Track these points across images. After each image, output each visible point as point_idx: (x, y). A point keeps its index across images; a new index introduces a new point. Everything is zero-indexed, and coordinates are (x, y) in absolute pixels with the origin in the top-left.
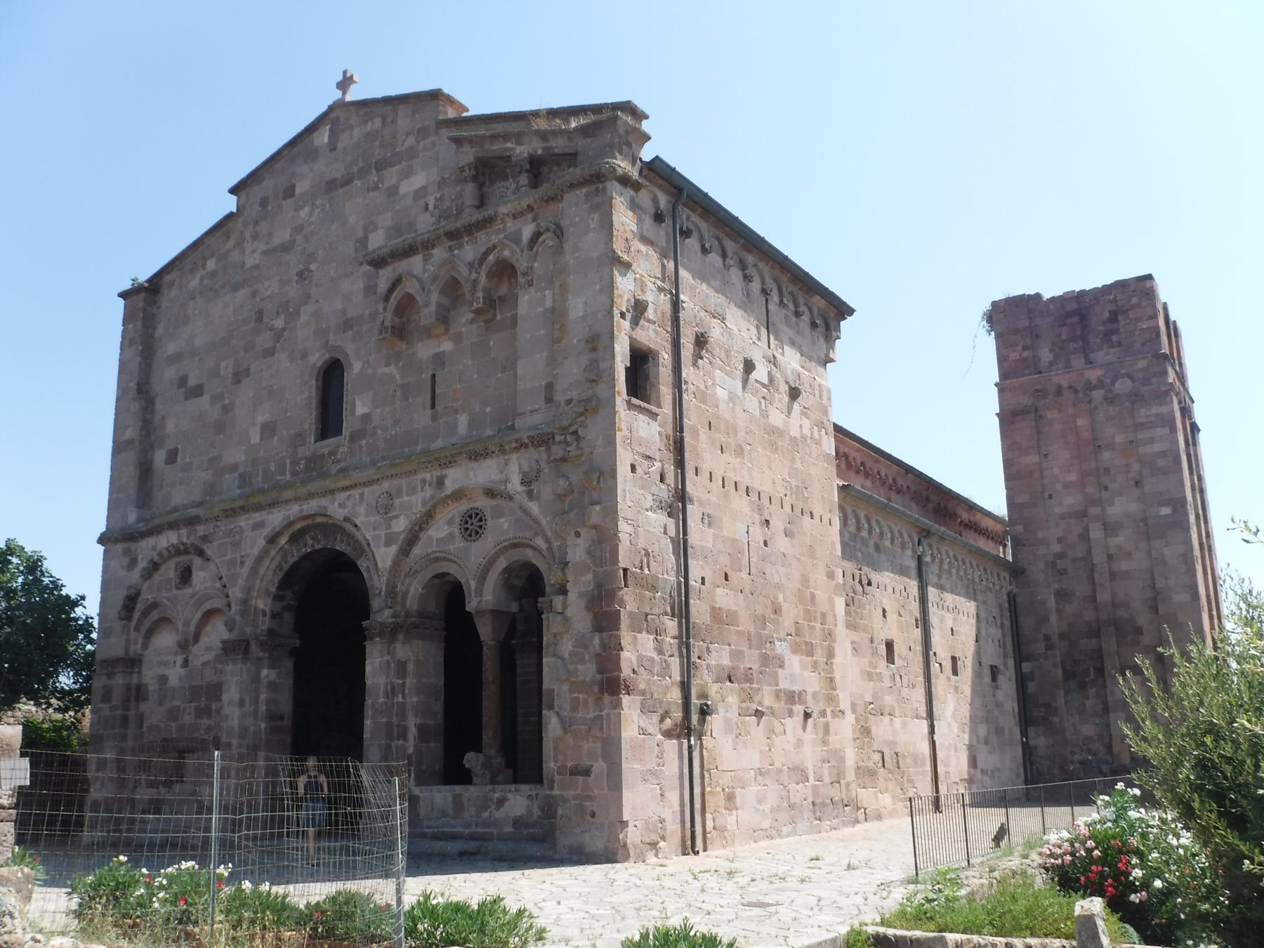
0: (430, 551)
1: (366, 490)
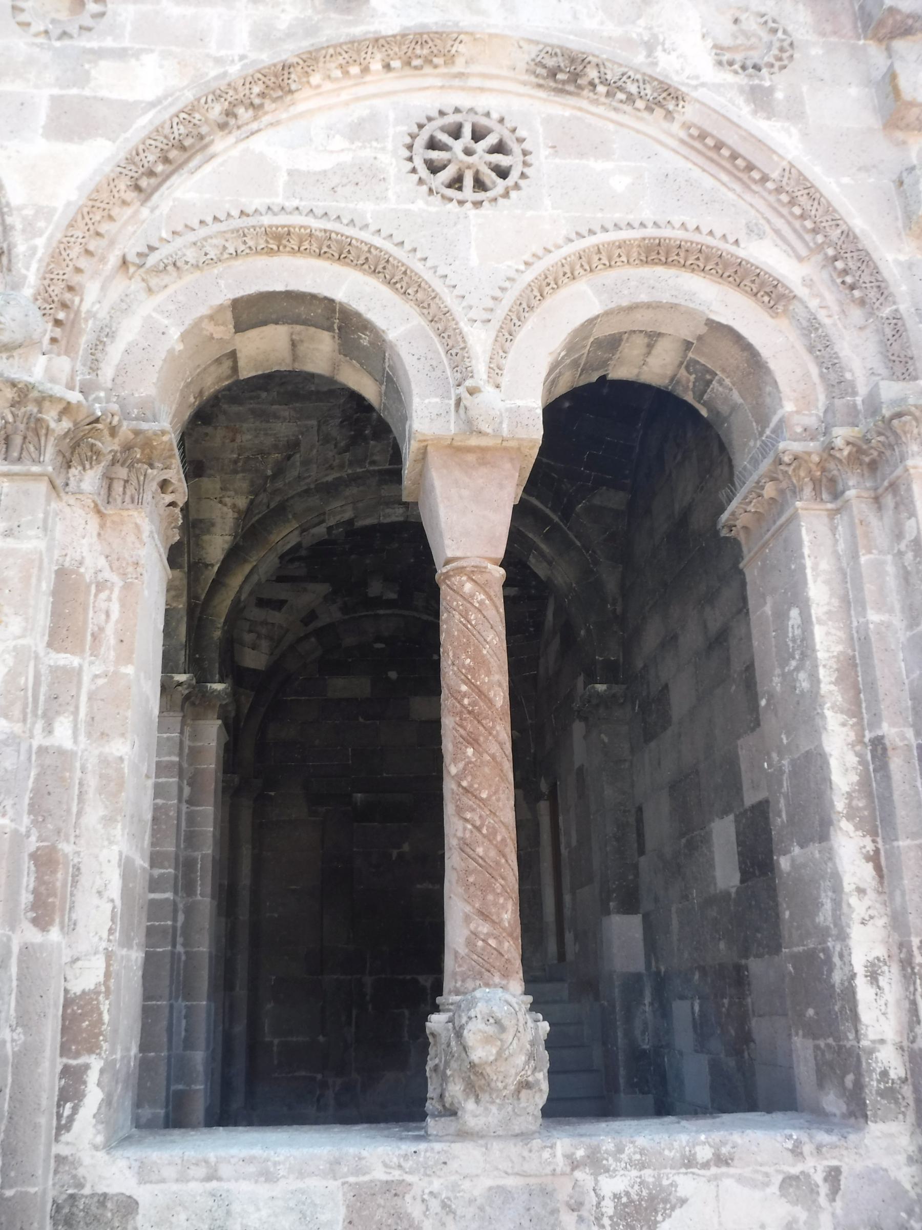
0: (258, 203)
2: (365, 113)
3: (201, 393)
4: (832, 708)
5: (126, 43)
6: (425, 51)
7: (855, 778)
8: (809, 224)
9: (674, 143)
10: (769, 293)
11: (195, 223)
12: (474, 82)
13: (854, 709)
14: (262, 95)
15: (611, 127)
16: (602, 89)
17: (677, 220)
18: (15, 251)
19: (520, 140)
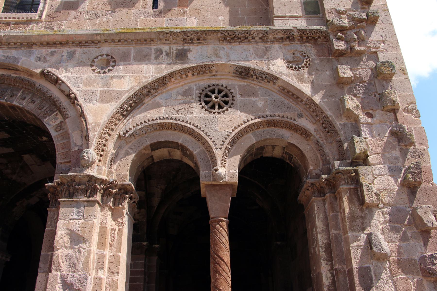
1: (79, 51)
2: (187, 88)
3: (143, 167)
4: (323, 259)
5: (121, 74)
6: (204, 70)
7: (330, 281)
8: (315, 114)
9: (276, 91)
10: (305, 134)
11: (139, 123)
12: (219, 77)
13: (330, 259)
14: (158, 86)
15: (258, 87)
16: (255, 77)
17: (277, 114)
18: (90, 136)
19: (232, 93)
